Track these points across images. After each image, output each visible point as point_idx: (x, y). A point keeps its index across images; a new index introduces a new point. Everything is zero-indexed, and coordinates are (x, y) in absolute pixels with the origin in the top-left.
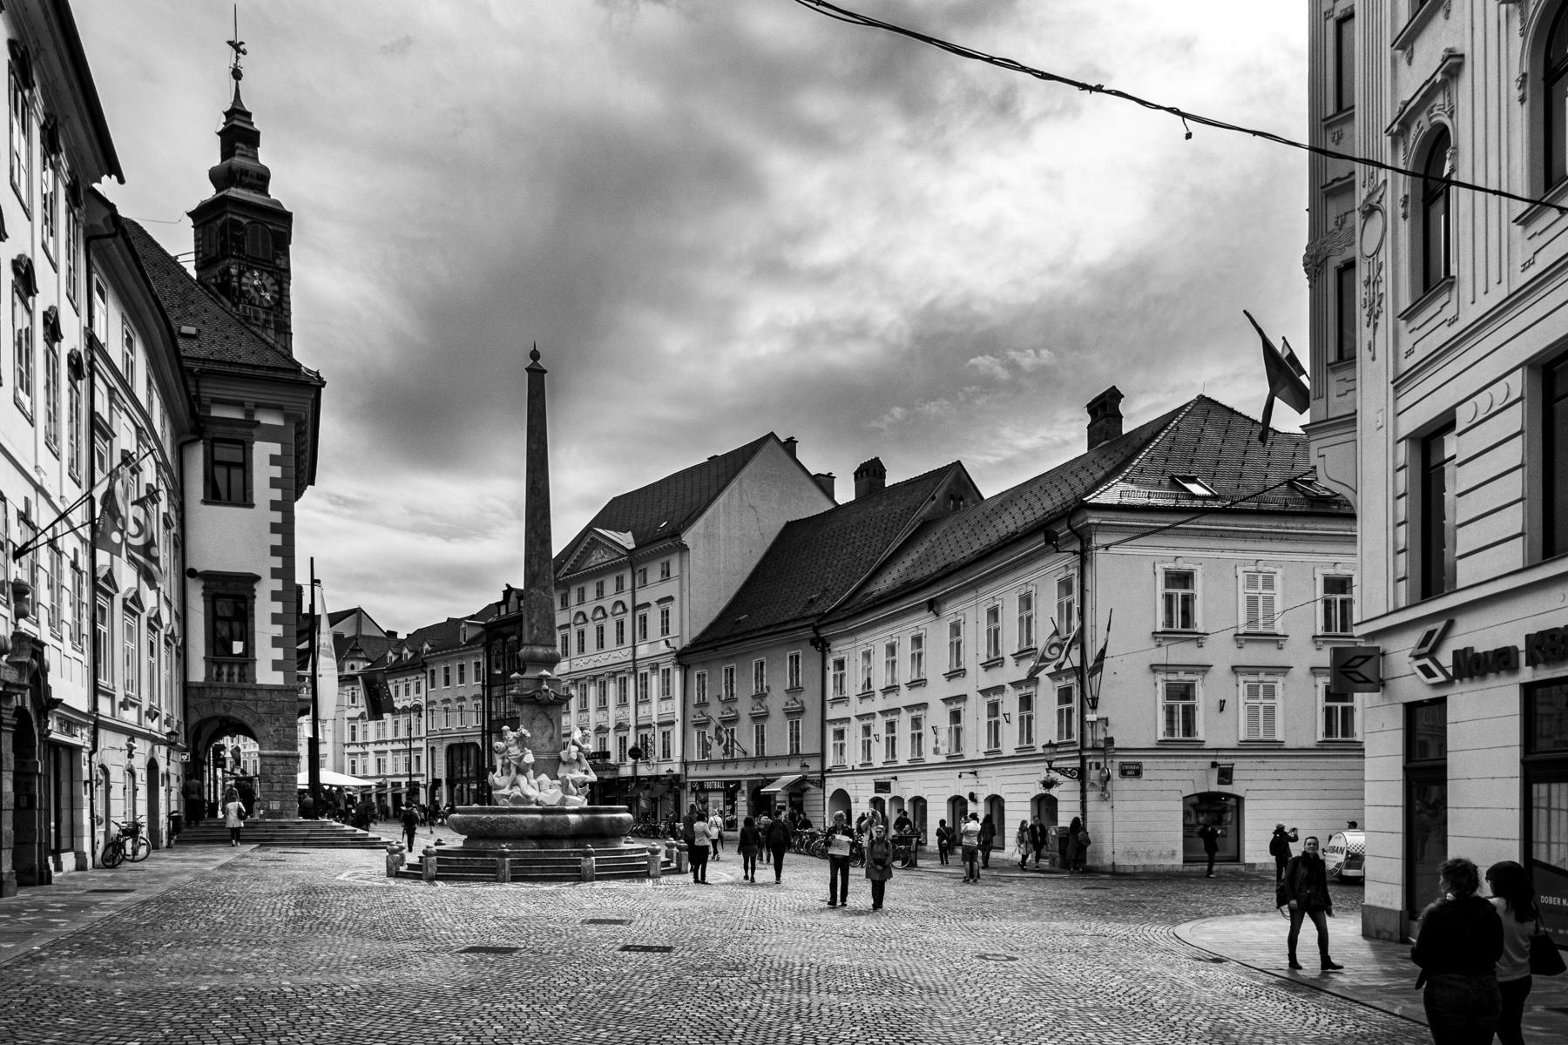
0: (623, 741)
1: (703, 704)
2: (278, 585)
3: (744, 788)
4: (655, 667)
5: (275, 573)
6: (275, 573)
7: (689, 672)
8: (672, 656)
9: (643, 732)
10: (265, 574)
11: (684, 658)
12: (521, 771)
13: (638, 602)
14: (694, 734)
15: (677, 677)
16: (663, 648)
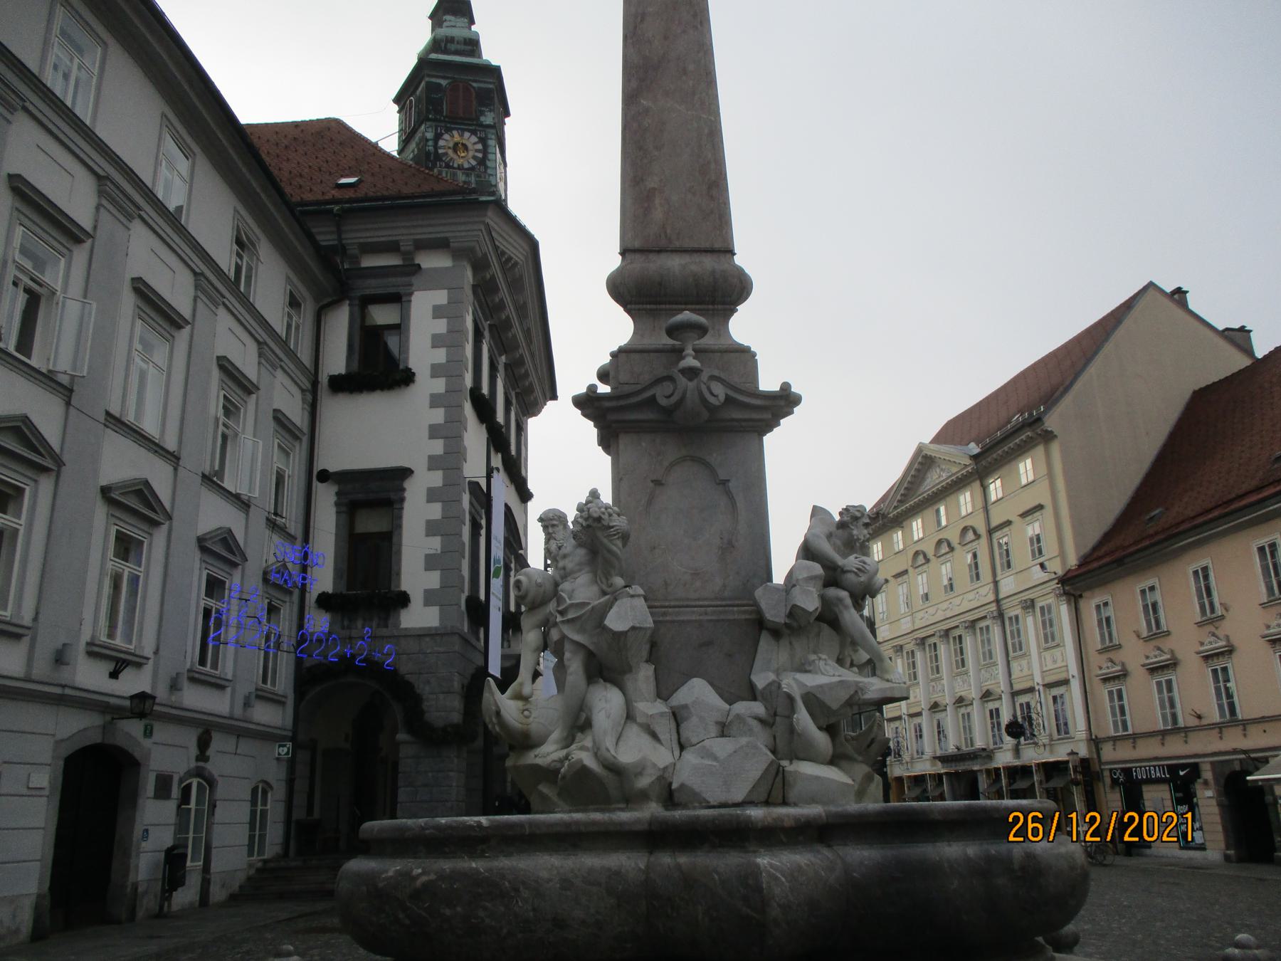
0: (995, 714)
1: (1111, 648)
2: (437, 479)
3: (1207, 774)
4: (1030, 605)
5: (434, 463)
6: (434, 463)
7: (1082, 603)
8: (1054, 585)
9: (1023, 699)
10: (418, 463)
11: (1073, 585)
12: (604, 666)
13: (994, 523)
14: (1102, 693)
15: (1063, 612)
16: (1038, 575)
